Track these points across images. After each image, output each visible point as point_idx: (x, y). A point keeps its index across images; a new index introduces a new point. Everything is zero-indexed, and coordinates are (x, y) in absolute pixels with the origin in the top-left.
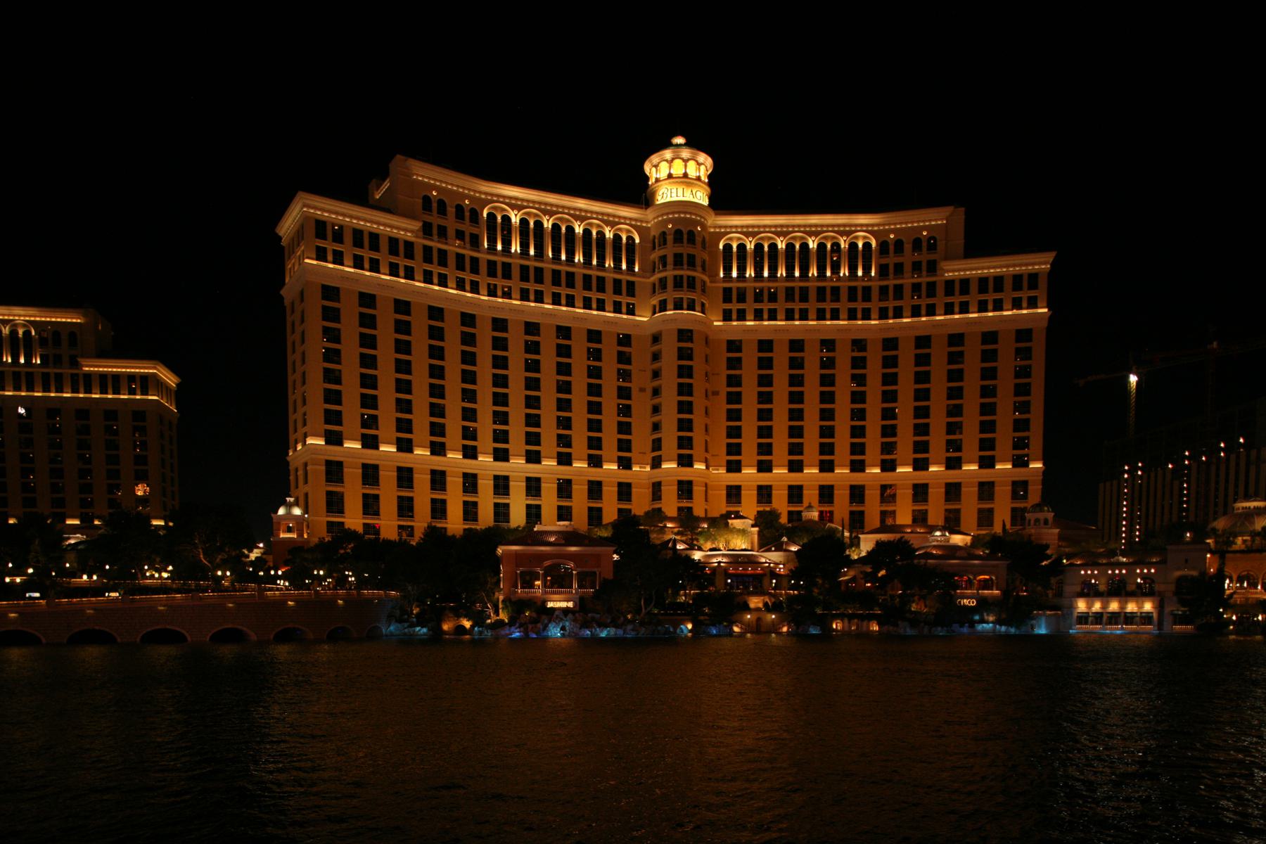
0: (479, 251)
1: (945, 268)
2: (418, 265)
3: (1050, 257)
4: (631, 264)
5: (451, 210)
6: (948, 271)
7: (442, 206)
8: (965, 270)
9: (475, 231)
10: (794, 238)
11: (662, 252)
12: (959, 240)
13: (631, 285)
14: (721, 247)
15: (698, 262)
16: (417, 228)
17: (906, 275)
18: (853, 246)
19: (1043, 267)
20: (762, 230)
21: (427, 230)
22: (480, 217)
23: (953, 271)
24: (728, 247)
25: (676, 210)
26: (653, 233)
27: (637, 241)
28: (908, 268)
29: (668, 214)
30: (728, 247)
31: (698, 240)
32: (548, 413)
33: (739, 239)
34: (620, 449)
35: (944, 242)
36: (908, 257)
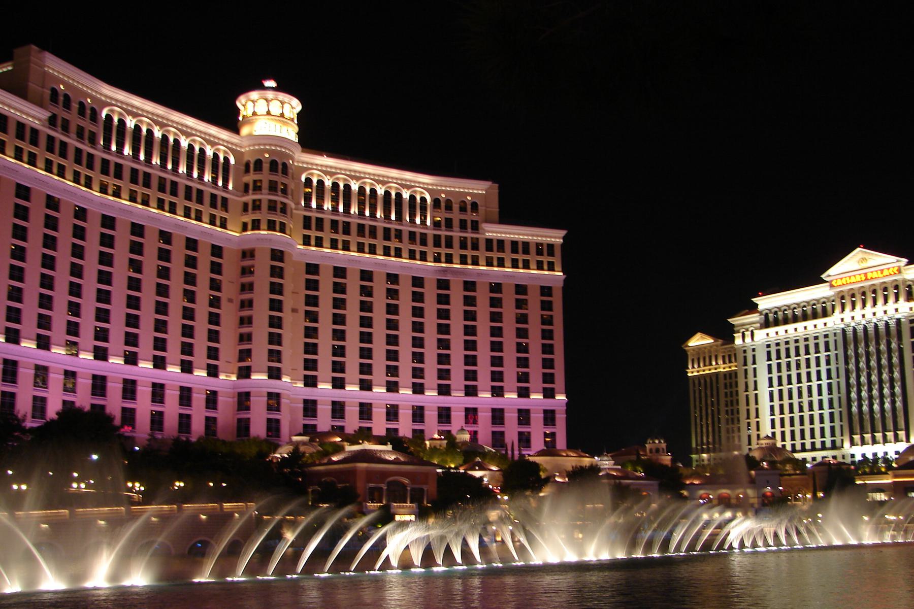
0: (95, 149)
1: (486, 229)
2: (41, 153)
3: (563, 233)
4: (226, 181)
5: (75, 106)
6: (489, 232)
7: (67, 100)
9: (93, 128)
11: (257, 177)
12: (494, 207)
14: (303, 179)
15: (289, 191)
17: (455, 229)
19: (558, 240)
20: (339, 171)
21: (52, 121)
22: (99, 117)
24: (308, 182)
26: (246, 158)
27: (232, 161)
28: (456, 223)
29: (265, 145)
30: (308, 182)
31: (290, 171)
32: (405, 349)
33: (319, 175)
34: (361, 373)
35: (484, 208)
36: (456, 216)
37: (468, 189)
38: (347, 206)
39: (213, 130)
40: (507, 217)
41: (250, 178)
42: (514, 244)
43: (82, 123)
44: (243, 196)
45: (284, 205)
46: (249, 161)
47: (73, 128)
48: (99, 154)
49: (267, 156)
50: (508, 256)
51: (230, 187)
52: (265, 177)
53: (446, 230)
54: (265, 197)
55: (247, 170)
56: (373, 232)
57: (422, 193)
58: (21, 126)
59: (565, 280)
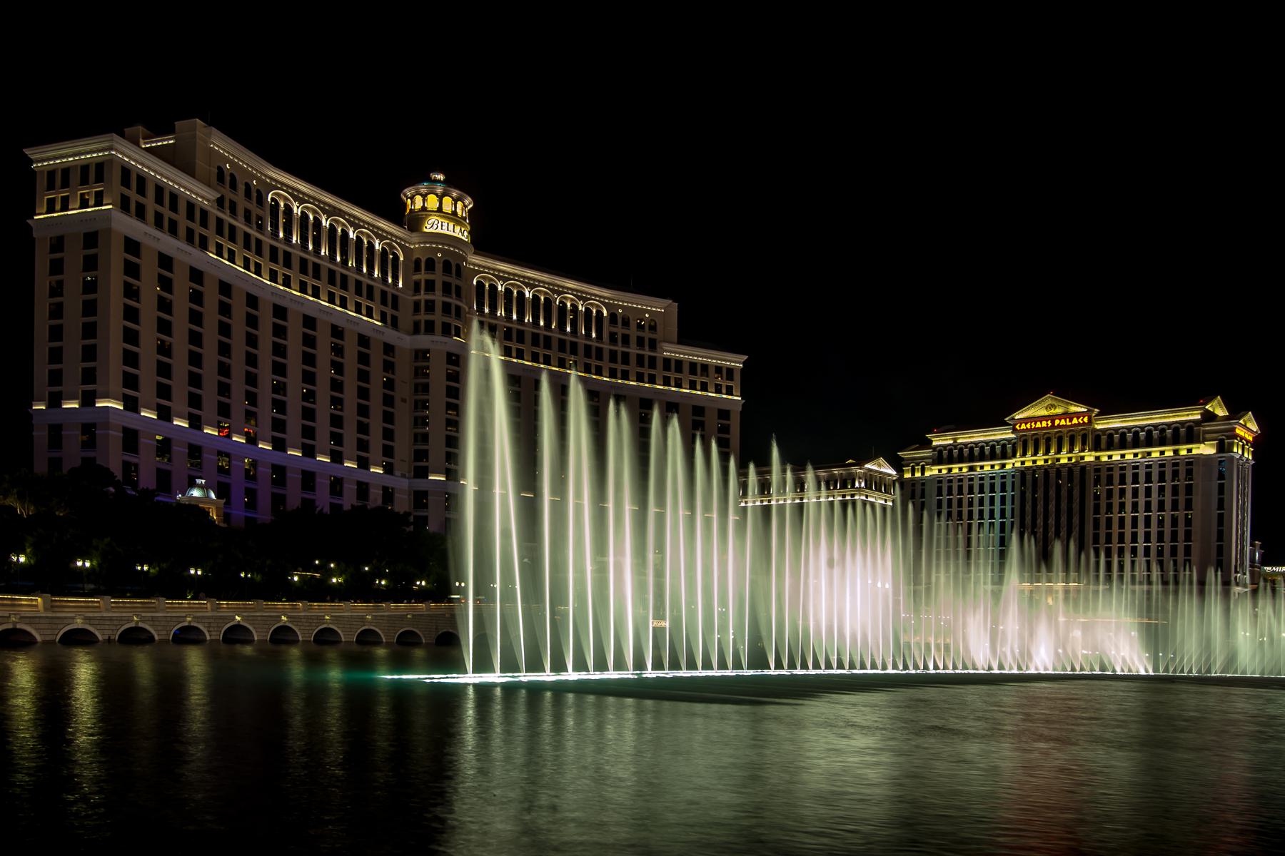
0: (263, 234)
1: (664, 348)
6: (667, 351)
8: (680, 353)
9: (260, 212)
10: (538, 291)
11: (430, 277)
13: (395, 298)
14: (475, 283)
15: (463, 293)
16: (214, 198)
18: (588, 311)
19: (738, 365)
21: (220, 202)
23: (671, 352)
25: (446, 242)
27: (402, 259)
28: (633, 340)
30: (480, 285)
37: (647, 306)
38: (521, 315)
39: (383, 224)
40: (686, 337)
41: (422, 276)
42: (693, 366)
43: (249, 206)
44: (415, 295)
45: (458, 309)
46: (420, 259)
47: (241, 212)
48: (267, 240)
49: (439, 255)
50: (686, 377)
51: (400, 285)
52: (438, 277)
53: (622, 346)
54: (438, 297)
55: (417, 268)
56: (548, 342)
57: (598, 306)
58: (191, 206)
59: (743, 405)
